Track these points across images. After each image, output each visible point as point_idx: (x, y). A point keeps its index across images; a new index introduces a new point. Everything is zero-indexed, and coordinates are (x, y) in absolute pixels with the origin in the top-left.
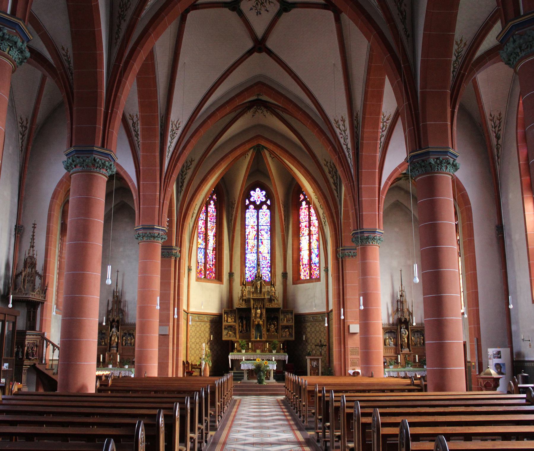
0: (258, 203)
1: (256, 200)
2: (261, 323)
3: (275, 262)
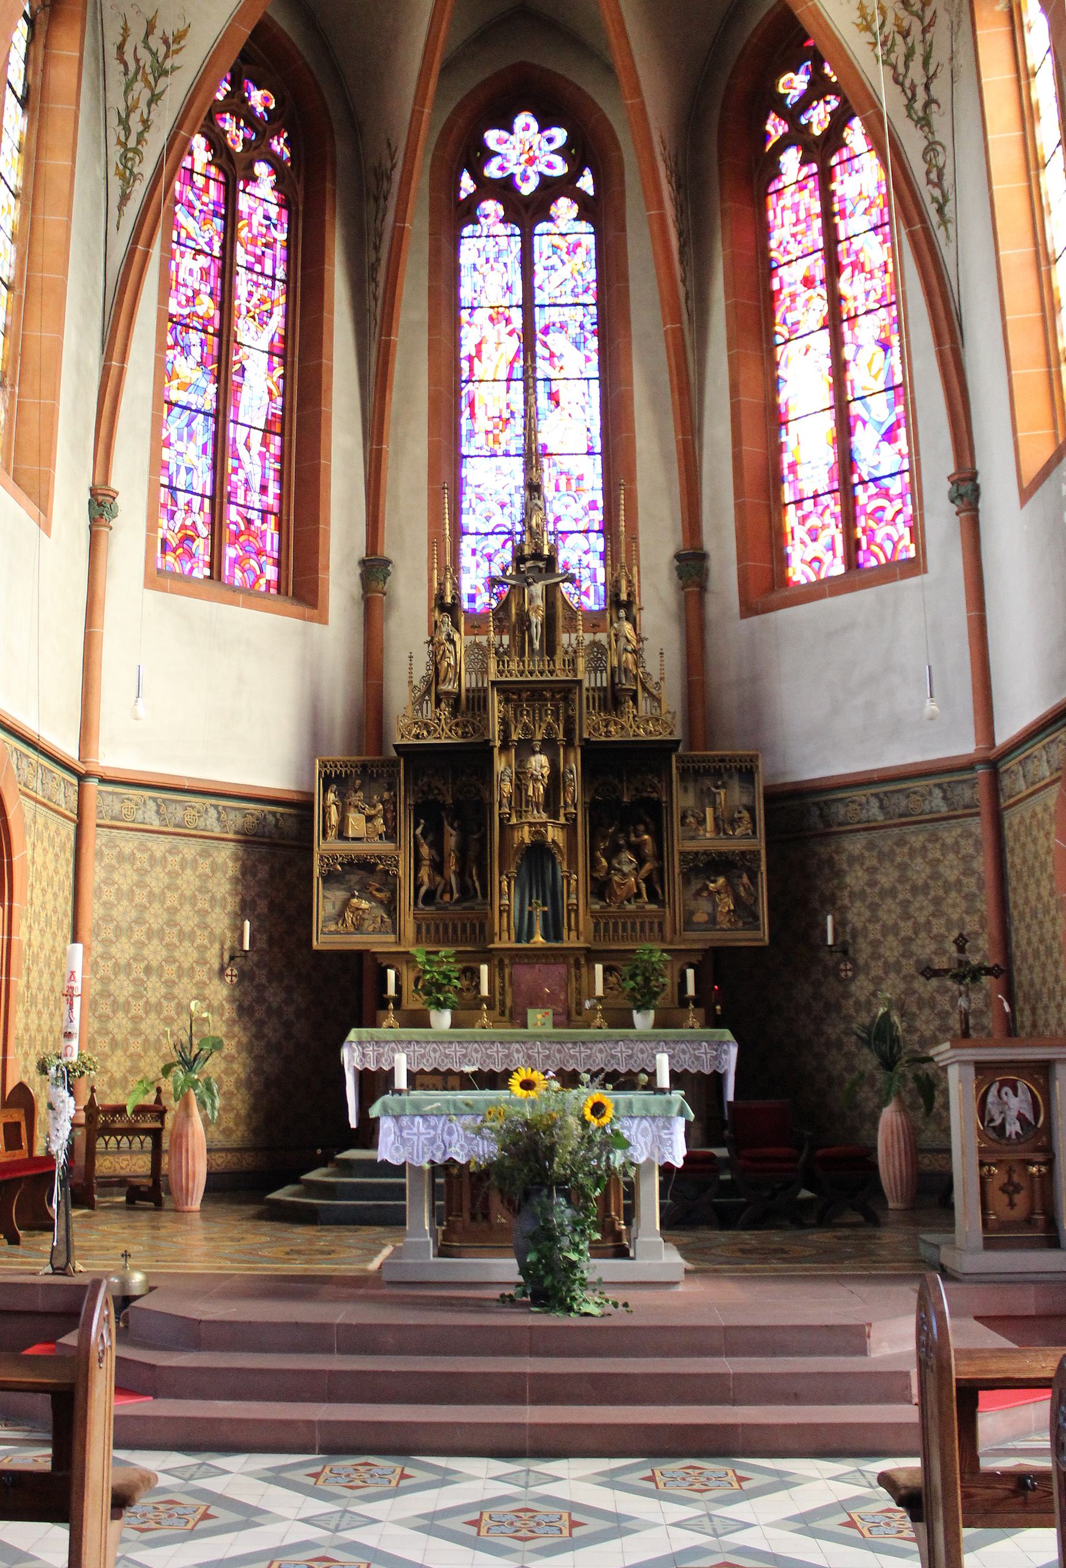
1: (518, 170)
2: (554, 834)
3: (631, 496)
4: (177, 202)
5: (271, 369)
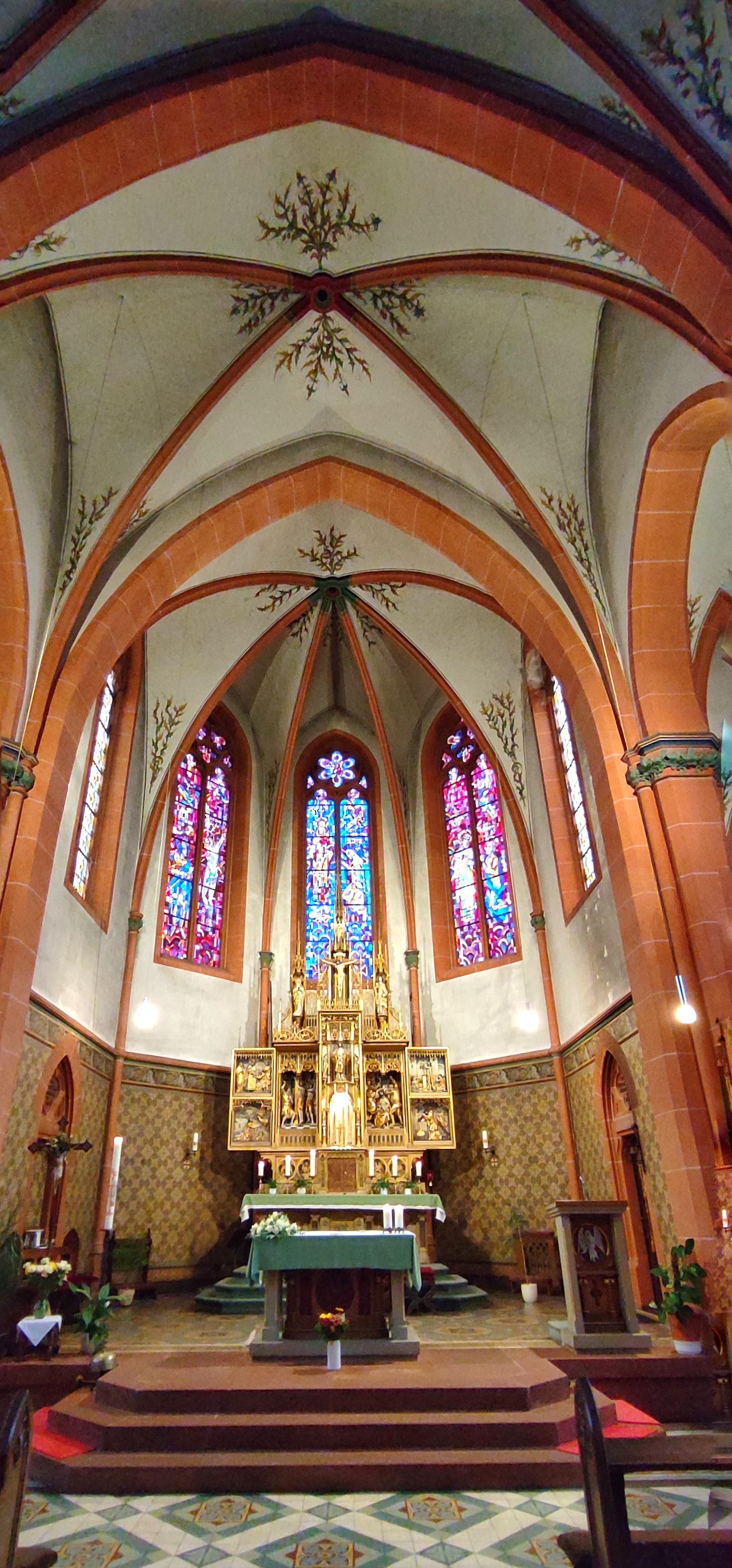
1: (333, 776)
4: (179, 783)
5: (219, 862)
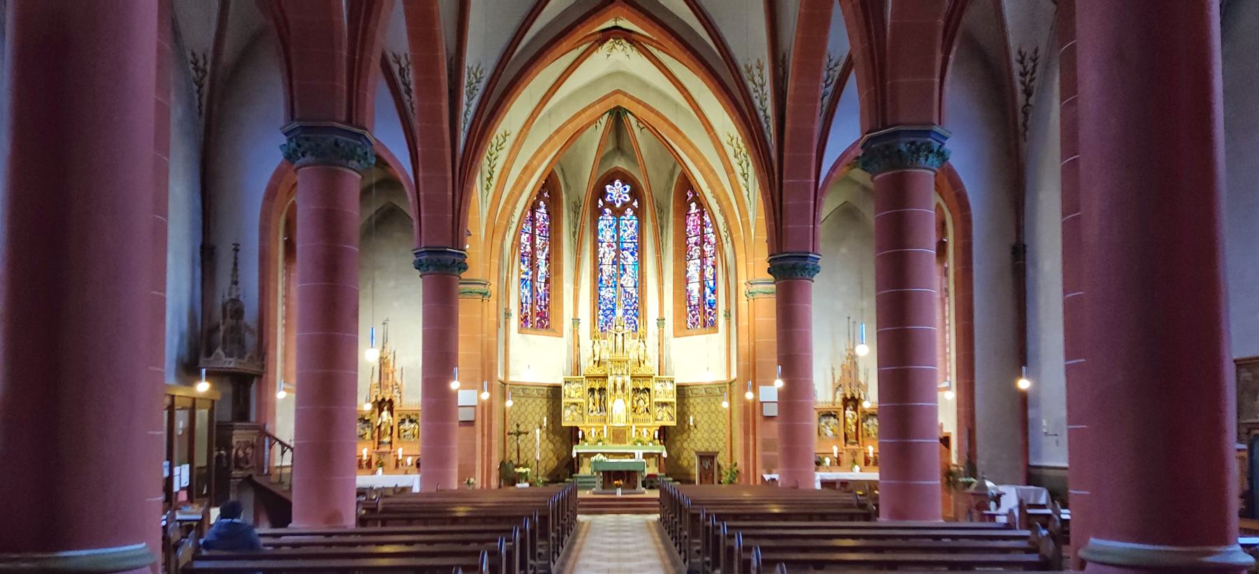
0: (618, 205)
